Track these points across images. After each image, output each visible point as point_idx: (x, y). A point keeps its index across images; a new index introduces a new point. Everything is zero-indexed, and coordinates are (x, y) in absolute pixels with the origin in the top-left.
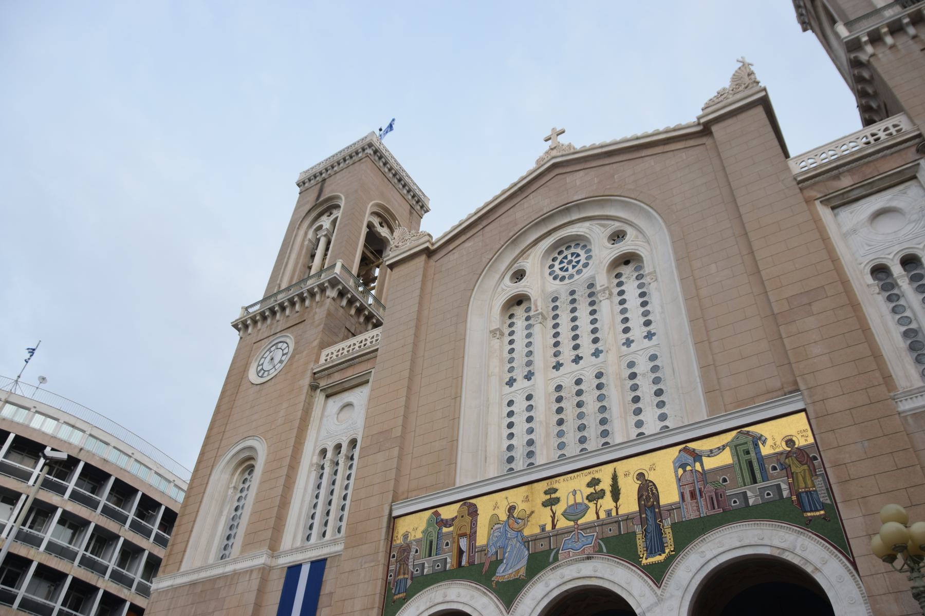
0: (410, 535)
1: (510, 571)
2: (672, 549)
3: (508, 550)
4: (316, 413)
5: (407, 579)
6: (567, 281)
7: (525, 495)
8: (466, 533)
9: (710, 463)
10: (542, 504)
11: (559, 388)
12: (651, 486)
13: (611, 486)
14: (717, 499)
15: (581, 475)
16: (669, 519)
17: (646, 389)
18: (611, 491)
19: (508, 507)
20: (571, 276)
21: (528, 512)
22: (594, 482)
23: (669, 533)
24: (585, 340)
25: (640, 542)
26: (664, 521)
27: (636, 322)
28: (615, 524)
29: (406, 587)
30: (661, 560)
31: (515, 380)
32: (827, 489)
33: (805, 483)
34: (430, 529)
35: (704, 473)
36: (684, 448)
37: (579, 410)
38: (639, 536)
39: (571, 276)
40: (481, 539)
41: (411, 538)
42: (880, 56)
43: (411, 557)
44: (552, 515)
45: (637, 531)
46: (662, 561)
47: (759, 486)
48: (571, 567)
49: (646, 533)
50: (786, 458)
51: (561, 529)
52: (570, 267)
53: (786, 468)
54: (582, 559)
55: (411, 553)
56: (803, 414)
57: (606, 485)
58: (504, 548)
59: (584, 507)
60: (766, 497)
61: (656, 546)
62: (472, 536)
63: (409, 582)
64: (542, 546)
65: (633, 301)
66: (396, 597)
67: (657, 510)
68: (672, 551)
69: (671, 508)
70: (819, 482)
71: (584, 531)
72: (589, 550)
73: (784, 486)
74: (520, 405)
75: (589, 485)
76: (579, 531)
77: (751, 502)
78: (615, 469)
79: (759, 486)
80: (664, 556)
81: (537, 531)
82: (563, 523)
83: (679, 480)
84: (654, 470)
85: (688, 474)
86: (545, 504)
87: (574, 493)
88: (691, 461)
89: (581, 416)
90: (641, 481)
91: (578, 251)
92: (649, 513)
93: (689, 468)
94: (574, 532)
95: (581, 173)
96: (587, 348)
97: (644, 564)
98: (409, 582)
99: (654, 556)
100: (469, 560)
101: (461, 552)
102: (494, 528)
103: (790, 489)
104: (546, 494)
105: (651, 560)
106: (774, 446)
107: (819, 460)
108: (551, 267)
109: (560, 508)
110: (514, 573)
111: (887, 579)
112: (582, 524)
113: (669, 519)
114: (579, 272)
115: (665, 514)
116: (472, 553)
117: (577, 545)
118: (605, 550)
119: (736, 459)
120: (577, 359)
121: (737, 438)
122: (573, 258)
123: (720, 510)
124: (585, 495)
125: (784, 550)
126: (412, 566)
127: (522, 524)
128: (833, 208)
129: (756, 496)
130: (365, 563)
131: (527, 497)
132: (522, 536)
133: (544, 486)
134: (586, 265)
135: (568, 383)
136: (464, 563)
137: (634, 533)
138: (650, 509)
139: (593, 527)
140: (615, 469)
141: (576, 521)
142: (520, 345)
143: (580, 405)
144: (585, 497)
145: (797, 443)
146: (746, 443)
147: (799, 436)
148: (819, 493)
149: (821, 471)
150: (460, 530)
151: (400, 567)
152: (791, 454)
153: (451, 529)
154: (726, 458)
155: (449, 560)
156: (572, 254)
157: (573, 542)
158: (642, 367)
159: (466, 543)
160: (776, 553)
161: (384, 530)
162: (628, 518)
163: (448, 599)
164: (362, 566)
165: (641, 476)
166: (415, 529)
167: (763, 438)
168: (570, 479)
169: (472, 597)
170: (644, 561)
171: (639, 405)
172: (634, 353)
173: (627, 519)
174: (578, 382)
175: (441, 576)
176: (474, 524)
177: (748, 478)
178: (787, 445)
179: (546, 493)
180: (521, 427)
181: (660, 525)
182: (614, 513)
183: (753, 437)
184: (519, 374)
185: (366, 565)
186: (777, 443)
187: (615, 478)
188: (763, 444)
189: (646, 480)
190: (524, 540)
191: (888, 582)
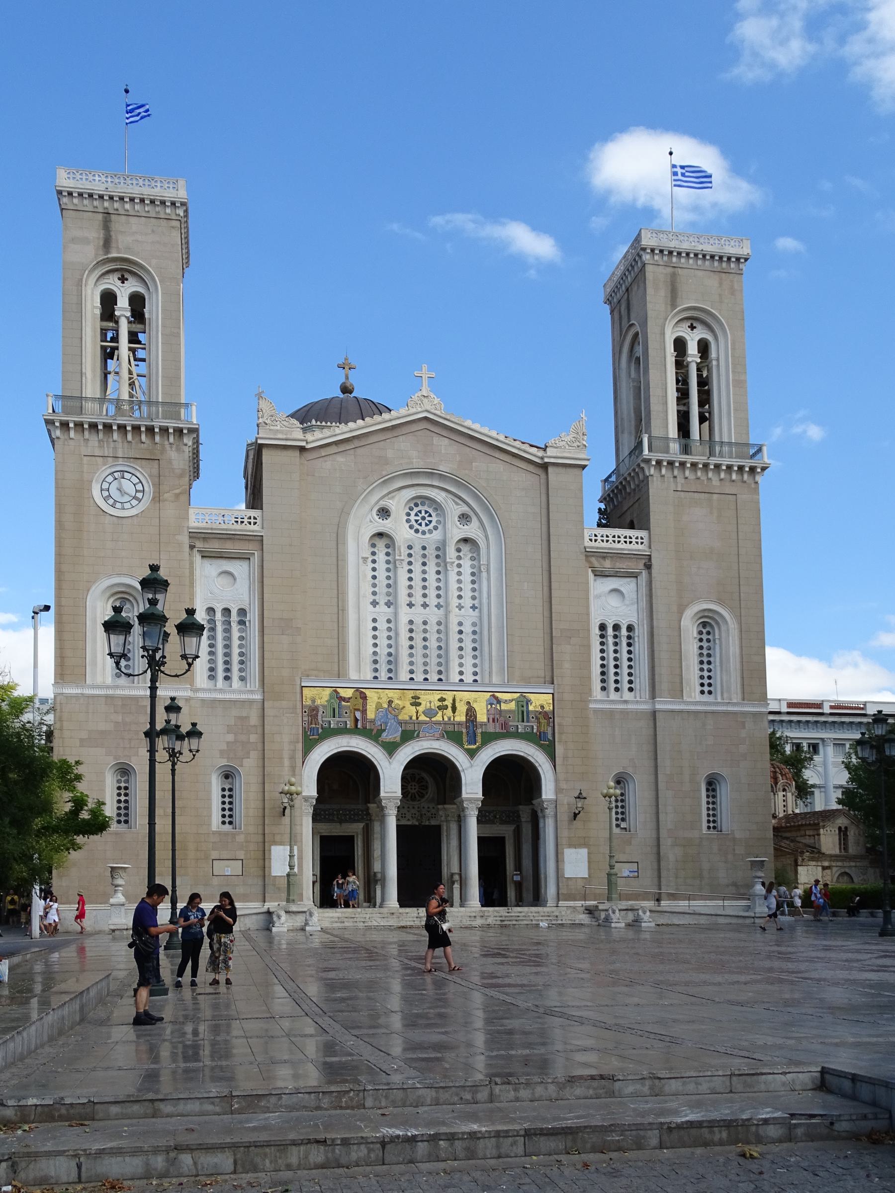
6: (419, 535)
9: (504, 707)
11: (411, 622)
14: (505, 725)
17: (468, 645)
20: (424, 533)
21: (401, 707)
22: (442, 700)
24: (432, 593)
25: (465, 738)
31: (378, 603)
34: (332, 701)
35: (501, 711)
37: (424, 643)
39: (424, 533)
40: (371, 715)
41: (318, 702)
49: (468, 733)
52: (423, 524)
53: (538, 718)
57: (449, 703)
58: (386, 723)
62: (364, 712)
63: (320, 731)
64: (410, 727)
70: (550, 730)
75: (439, 700)
77: (519, 731)
80: (474, 747)
82: (422, 718)
89: (425, 647)
91: (430, 511)
93: (493, 706)
95: (446, 441)
96: (432, 601)
98: (320, 731)
101: (356, 720)
109: (421, 709)
114: (430, 532)
115: (479, 726)
120: (425, 605)
121: (519, 697)
122: (426, 516)
124: (437, 705)
128: (595, 575)
132: (398, 719)
135: (418, 620)
136: (359, 726)
141: (431, 718)
143: (425, 639)
154: (512, 706)
155: (348, 722)
156: (426, 512)
162: (459, 724)
165: (468, 703)
171: (462, 653)
172: (463, 616)
174: (425, 623)
176: (365, 705)
177: (520, 720)
179: (413, 698)
182: (452, 719)
184: (382, 599)
185: (288, 715)
187: (454, 700)
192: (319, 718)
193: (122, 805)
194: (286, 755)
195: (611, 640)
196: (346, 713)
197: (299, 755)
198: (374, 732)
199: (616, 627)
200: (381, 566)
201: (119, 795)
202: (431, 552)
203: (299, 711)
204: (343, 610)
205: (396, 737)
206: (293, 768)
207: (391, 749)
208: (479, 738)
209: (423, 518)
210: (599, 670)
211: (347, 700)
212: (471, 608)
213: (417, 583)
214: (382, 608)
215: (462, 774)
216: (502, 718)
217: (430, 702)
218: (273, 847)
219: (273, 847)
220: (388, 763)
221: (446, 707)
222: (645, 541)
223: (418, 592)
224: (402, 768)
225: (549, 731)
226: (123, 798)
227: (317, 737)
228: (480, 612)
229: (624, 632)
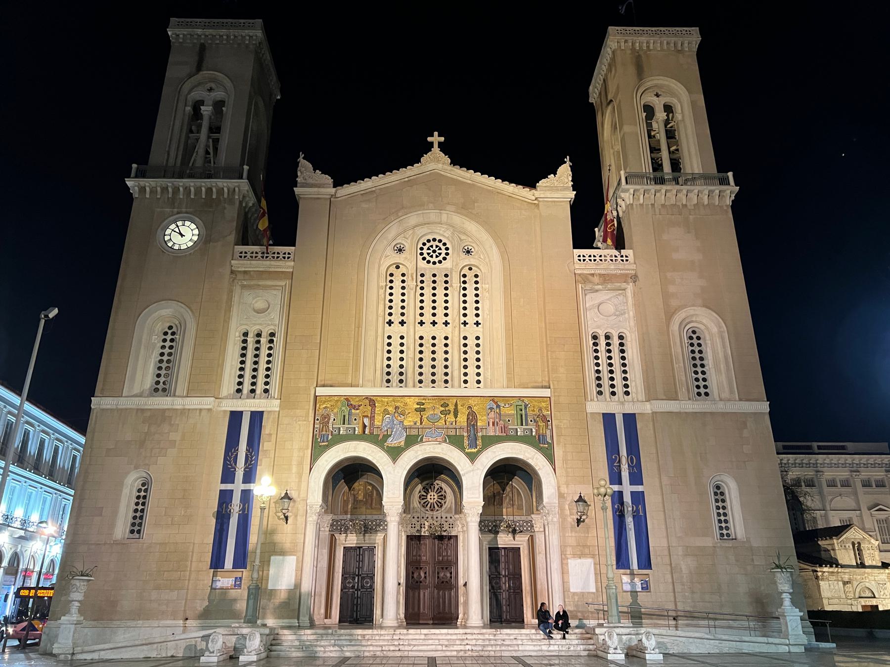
1: (395, 442)
4: (236, 299)
14: (504, 429)
17: (471, 356)
20: (434, 263)
24: (440, 311)
25: (466, 442)
27: (471, 312)
34: (343, 408)
38: (465, 438)
39: (434, 263)
42: (634, 206)
52: (434, 255)
57: (451, 408)
58: (392, 428)
61: (473, 444)
62: (372, 418)
64: (414, 432)
65: (471, 298)
66: (321, 444)
70: (548, 432)
73: (534, 430)
74: (396, 341)
77: (519, 434)
80: (476, 450)
81: (412, 423)
85: (493, 412)
86: (416, 410)
96: (440, 319)
98: (330, 437)
101: (365, 426)
105: (469, 450)
106: (533, 411)
108: (422, 249)
112: (437, 425)
114: (440, 262)
115: (479, 430)
120: (434, 323)
134: (445, 259)
142: (397, 298)
151: (323, 427)
153: (358, 411)
155: (356, 429)
156: (437, 246)
158: (471, 342)
165: (470, 407)
170: (467, 450)
175: (351, 437)
176: (373, 411)
177: (519, 423)
180: (395, 355)
184: (397, 319)
192: (330, 426)
193: (138, 514)
194: (294, 463)
195: (602, 347)
196: (355, 420)
198: (381, 437)
199: (607, 337)
200: (397, 291)
201: (137, 504)
202: (440, 279)
203: (311, 419)
204: (358, 328)
205: (400, 442)
206: (300, 475)
207: (395, 453)
208: (479, 442)
209: (434, 251)
210: (594, 375)
212: (475, 324)
213: (428, 304)
214: (396, 326)
215: (463, 478)
216: (502, 422)
217: (434, 408)
218: (272, 558)
222: (631, 258)
223: (428, 311)
224: (405, 473)
225: (548, 432)
226: (140, 507)
227: (327, 443)
228: (483, 327)
229: (616, 341)
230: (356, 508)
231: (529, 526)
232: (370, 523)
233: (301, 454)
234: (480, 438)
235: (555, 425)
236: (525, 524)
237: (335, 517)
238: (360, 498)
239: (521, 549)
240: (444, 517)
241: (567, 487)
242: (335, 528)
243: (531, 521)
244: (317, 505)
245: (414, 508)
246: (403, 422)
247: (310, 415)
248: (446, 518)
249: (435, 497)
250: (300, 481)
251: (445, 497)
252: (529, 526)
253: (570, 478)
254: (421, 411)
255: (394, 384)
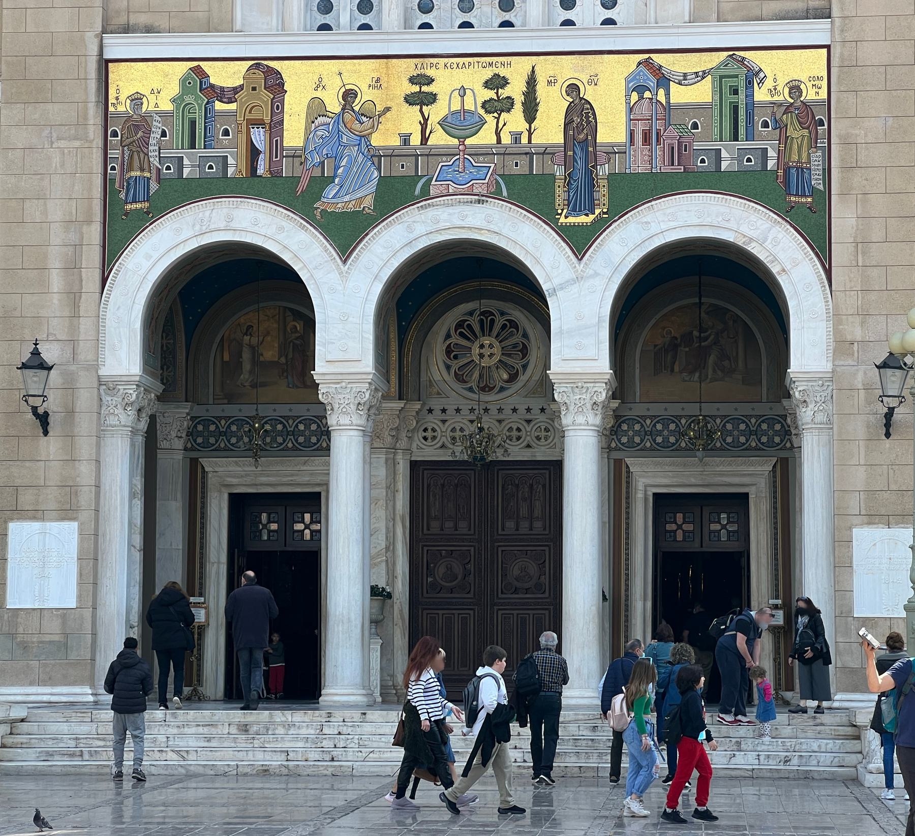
0: (145, 100)
1: (347, 198)
2: (605, 210)
3: (343, 164)
5: (149, 179)
7: (376, 75)
8: (263, 120)
9: (680, 95)
10: (405, 98)
12: (588, 109)
13: (524, 94)
15: (476, 64)
16: (607, 165)
18: (523, 103)
19: (343, 90)
21: (380, 108)
22: (497, 82)
23: (604, 186)
25: (560, 194)
26: (599, 167)
28: (524, 156)
29: (148, 193)
30: (587, 223)
32: (824, 169)
33: (800, 156)
34: (189, 99)
35: (668, 107)
36: (647, 60)
38: (559, 183)
43: (152, 141)
44: (422, 122)
45: (558, 174)
46: (589, 224)
47: (739, 145)
48: (450, 210)
49: (569, 179)
50: (783, 114)
51: (437, 147)
53: (780, 126)
54: (469, 200)
55: (152, 135)
56: (825, 51)
57: (516, 90)
58: (336, 158)
59: (478, 119)
60: (745, 163)
62: (275, 127)
63: (154, 186)
66: (129, 207)
67: (591, 149)
68: (604, 213)
69: (612, 151)
70: (817, 158)
71: (475, 158)
72: (480, 187)
73: (772, 153)
75: (488, 84)
76: (466, 156)
77: (724, 165)
78: (533, 68)
79: (739, 145)
80: (592, 217)
81: (396, 142)
82: (439, 138)
83: (631, 109)
84: (596, 85)
85: (646, 103)
86: (410, 100)
87: (462, 92)
88: (652, 84)
90: (572, 98)
92: (578, 151)
93: (647, 94)
94: (458, 157)
97: (562, 223)
98: (154, 186)
99: (578, 215)
100: (270, 168)
101: (254, 153)
102: (316, 121)
103: (778, 159)
104: (413, 84)
105: (572, 220)
106: (774, 91)
107: (826, 127)
109: (436, 113)
110: (353, 202)
111: (860, 298)
112: (473, 147)
113: (607, 165)
115: (602, 157)
116: (276, 157)
117: (461, 178)
118: (505, 193)
119: (717, 98)
121: (725, 64)
123: (681, 169)
124: (480, 102)
125: (751, 240)
126: (157, 159)
127: (369, 126)
129: (732, 159)
130: (59, 139)
131: (378, 80)
132: (369, 145)
133: (408, 68)
136: (260, 172)
137: (554, 175)
138: (581, 144)
139: (489, 154)
140: (533, 68)
141: (462, 139)
144: (479, 105)
145: (804, 94)
146: (737, 76)
147: (809, 85)
148: (812, 172)
149: (823, 143)
150: (250, 112)
151: (131, 157)
152: (792, 109)
153: (233, 106)
155: (231, 161)
157: (456, 171)
159: (263, 138)
160: (740, 242)
161: (92, 85)
162: (546, 151)
163: (234, 225)
164: (52, 143)
165: (573, 89)
166: (156, 91)
167: (762, 75)
168: (455, 66)
169: (281, 229)
170: (562, 220)
173: (544, 153)
176: (278, 107)
178: (790, 93)
179: (412, 80)
181: (592, 172)
182: (524, 140)
183: (749, 70)
185: (62, 144)
186: (779, 88)
187: (531, 82)
188: (758, 84)
189: (581, 99)
190: (372, 153)
191: (860, 302)
194: (55, 262)
196: (226, 133)
197: (92, 256)
198: (304, 184)
203: (94, 132)
206: (73, 297)
208: (602, 193)
211: (223, 94)
217: (463, 91)
218: (12, 526)
219: (12, 526)
220: (335, 275)
221: (507, 105)
224: (378, 288)
230: (263, 385)
231: (777, 433)
232: (301, 427)
233: (73, 237)
234: (601, 182)
235: (839, 137)
236: (764, 426)
237: (200, 411)
238: (270, 354)
239: (752, 497)
240: (522, 409)
241: (863, 323)
242: (200, 440)
243: (784, 417)
244: (128, 383)
245: (431, 383)
246: (366, 137)
247: (91, 122)
248: (528, 410)
249: (495, 350)
250: (75, 315)
251: (525, 351)
252: (777, 433)
253: (873, 296)
254: (422, 104)
255: (345, 19)
